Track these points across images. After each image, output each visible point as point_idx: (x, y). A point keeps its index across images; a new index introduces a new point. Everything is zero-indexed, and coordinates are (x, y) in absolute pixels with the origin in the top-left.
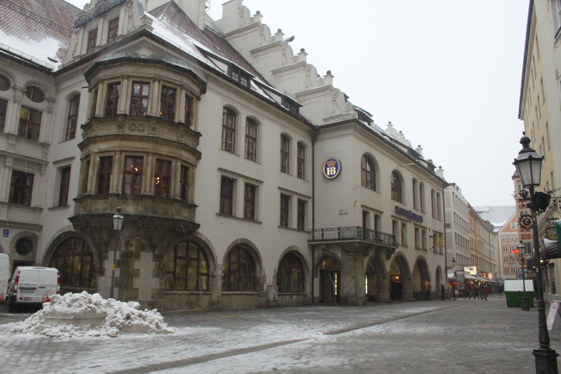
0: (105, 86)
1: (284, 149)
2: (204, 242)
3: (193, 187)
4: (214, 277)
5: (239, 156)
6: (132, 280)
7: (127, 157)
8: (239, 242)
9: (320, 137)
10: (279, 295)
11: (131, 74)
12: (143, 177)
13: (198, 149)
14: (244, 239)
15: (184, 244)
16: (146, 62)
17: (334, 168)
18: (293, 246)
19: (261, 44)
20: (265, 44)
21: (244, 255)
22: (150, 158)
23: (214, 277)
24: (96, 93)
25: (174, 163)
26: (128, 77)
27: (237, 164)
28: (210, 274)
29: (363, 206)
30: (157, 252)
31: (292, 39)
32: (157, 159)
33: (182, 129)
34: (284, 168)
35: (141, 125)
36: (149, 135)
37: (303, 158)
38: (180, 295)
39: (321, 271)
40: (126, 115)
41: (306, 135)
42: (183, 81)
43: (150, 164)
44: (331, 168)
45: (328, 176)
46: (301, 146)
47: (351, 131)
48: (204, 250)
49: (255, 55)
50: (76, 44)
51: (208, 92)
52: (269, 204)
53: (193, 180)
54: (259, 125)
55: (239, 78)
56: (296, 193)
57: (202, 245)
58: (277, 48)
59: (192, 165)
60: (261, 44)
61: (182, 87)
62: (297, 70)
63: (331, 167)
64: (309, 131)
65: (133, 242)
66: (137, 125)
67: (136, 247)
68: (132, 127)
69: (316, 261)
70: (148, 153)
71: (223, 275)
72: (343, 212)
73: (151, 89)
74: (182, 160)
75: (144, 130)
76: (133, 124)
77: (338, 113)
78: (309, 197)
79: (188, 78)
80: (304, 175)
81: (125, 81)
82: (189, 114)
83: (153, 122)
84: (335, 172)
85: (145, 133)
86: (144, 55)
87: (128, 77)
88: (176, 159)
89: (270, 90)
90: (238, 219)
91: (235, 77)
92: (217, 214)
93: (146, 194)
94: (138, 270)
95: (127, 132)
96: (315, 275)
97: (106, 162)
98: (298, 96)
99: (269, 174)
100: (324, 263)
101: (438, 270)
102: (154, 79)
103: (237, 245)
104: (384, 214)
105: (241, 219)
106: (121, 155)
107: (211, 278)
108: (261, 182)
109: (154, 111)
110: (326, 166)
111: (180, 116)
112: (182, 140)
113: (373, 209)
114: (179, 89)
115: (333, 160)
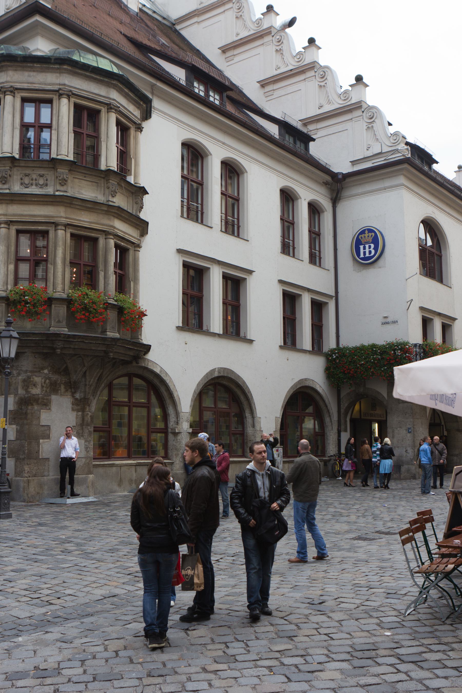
1: (286, 216)
2: (157, 376)
3: (136, 280)
4: (176, 434)
5: (211, 228)
6: (38, 444)
7: (19, 232)
8: (216, 374)
9: (346, 193)
10: (284, 462)
11: (18, 85)
12: (51, 267)
13: (143, 215)
14: (225, 369)
15: (124, 380)
16: (43, 62)
17: (372, 246)
18: (306, 379)
19: (238, 34)
20: (244, 34)
21: (225, 395)
22: (61, 233)
23: (176, 434)
25: (101, 242)
26: (13, 91)
27: (209, 241)
28: (170, 430)
29: (422, 309)
30: (77, 396)
31: (292, 23)
32: (72, 235)
33: (113, 182)
34: (288, 248)
35: (41, 176)
36: (57, 193)
37: (317, 230)
38: (121, 466)
39: (353, 421)
40: (13, 157)
41: (323, 190)
42: (112, 96)
43: (60, 243)
44: (367, 246)
45: (362, 259)
46: (314, 209)
47: (402, 180)
48: (157, 388)
49: (229, 54)
51: (154, 115)
52: (263, 310)
53: (136, 270)
54: (243, 173)
55: (207, 92)
56: (309, 290)
57: (156, 382)
58: (267, 39)
59: (133, 243)
60: (238, 34)
61: (110, 107)
62: (302, 77)
63: (367, 243)
64: (326, 184)
65: (38, 379)
66: (34, 177)
67: (42, 387)
68: (27, 181)
69: (345, 405)
70: (56, 225)
71: (191, 430)
72: (389, 320)
73: (54, 112)
74: (117, 236)
75: (47, 185)
76: (27, 175)
77: (377, 150)
78: (330, 297)
79: (120, 91)
80: (320, 258)
81: (9, 98)
82: (124, 156)
83: (63, 171)
84: (373, 252)
85: (50, 190)
86: (37, 50)
87: (13, 91)
88: (106, 233)
90: (214, 335)
91: (199, 89)
92: (178, 328)
93: (57, 295)
94: (49, 426)
95: (17, 188)
96: (343, 427)
98: (306, 122)
99: (262, 258)
100: (357, 407)
102: (60, 93)
103: (213, 379)
104: (457, 321)
105: (219, 335)
106: (9, 229)
107: (171, 437)
108: (250, 272)
109: (64, 151)
110: (358, 243)
111: (109, 159)
112: (114, 200)
113: (439, 314)
114: (104, 110)
115: (370, 231)
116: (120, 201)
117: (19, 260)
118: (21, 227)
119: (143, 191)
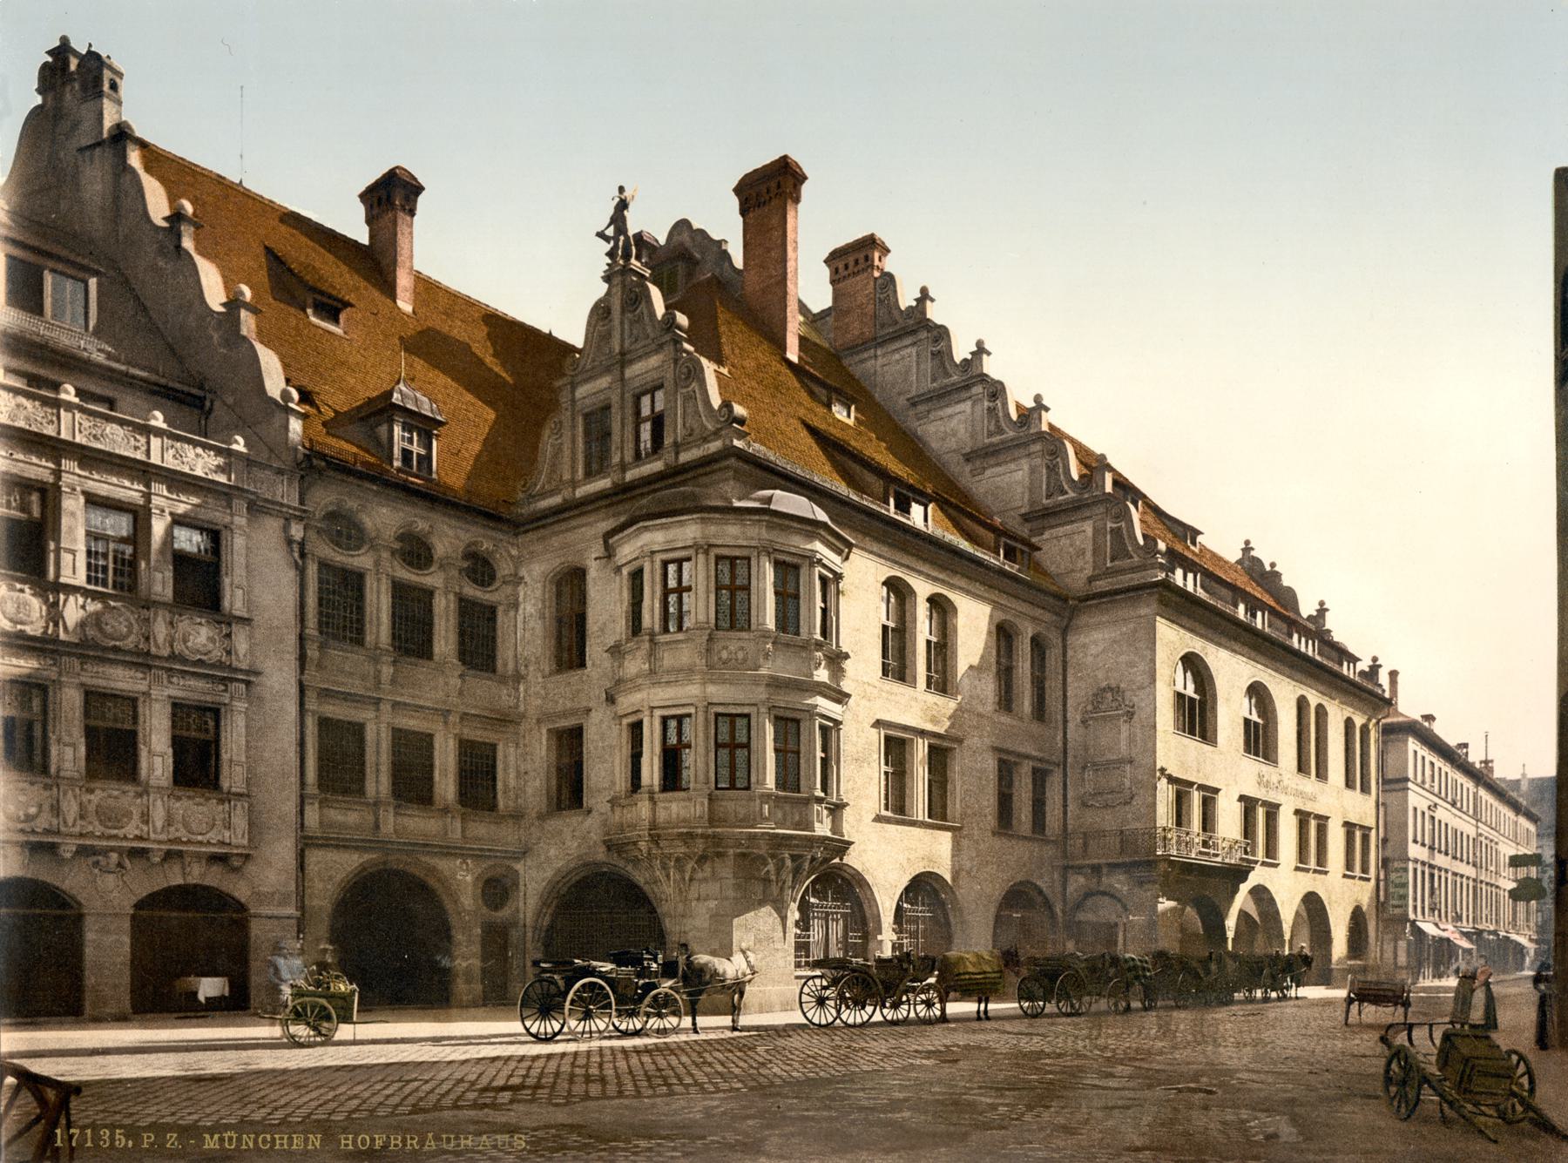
0: (658, 565)
13: (846, 686)
24: (637, 576)
35: (742, 648)
46: (1038, 644)
50: (558, 451)
89: (962, 511)
97: (673, 724)
101: (1357, 918)
116: (822, 675)
117: (718, 746)
118: (720, 710)
119: (847, 656)
